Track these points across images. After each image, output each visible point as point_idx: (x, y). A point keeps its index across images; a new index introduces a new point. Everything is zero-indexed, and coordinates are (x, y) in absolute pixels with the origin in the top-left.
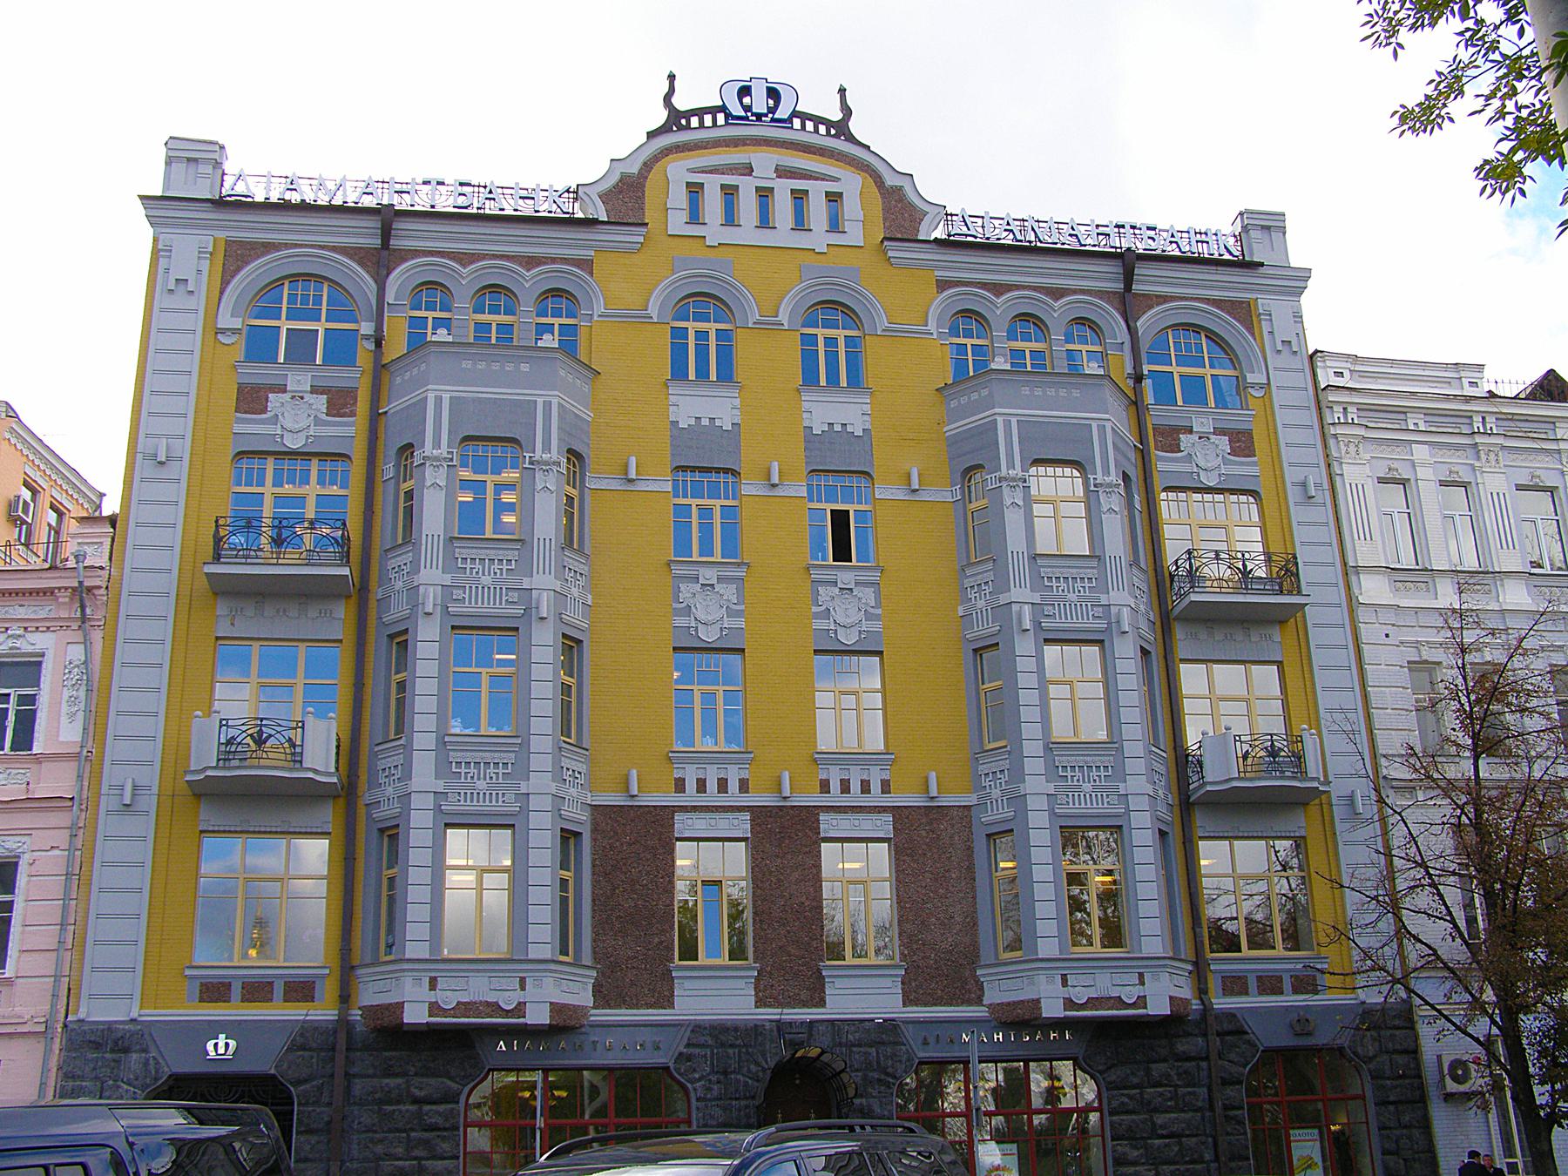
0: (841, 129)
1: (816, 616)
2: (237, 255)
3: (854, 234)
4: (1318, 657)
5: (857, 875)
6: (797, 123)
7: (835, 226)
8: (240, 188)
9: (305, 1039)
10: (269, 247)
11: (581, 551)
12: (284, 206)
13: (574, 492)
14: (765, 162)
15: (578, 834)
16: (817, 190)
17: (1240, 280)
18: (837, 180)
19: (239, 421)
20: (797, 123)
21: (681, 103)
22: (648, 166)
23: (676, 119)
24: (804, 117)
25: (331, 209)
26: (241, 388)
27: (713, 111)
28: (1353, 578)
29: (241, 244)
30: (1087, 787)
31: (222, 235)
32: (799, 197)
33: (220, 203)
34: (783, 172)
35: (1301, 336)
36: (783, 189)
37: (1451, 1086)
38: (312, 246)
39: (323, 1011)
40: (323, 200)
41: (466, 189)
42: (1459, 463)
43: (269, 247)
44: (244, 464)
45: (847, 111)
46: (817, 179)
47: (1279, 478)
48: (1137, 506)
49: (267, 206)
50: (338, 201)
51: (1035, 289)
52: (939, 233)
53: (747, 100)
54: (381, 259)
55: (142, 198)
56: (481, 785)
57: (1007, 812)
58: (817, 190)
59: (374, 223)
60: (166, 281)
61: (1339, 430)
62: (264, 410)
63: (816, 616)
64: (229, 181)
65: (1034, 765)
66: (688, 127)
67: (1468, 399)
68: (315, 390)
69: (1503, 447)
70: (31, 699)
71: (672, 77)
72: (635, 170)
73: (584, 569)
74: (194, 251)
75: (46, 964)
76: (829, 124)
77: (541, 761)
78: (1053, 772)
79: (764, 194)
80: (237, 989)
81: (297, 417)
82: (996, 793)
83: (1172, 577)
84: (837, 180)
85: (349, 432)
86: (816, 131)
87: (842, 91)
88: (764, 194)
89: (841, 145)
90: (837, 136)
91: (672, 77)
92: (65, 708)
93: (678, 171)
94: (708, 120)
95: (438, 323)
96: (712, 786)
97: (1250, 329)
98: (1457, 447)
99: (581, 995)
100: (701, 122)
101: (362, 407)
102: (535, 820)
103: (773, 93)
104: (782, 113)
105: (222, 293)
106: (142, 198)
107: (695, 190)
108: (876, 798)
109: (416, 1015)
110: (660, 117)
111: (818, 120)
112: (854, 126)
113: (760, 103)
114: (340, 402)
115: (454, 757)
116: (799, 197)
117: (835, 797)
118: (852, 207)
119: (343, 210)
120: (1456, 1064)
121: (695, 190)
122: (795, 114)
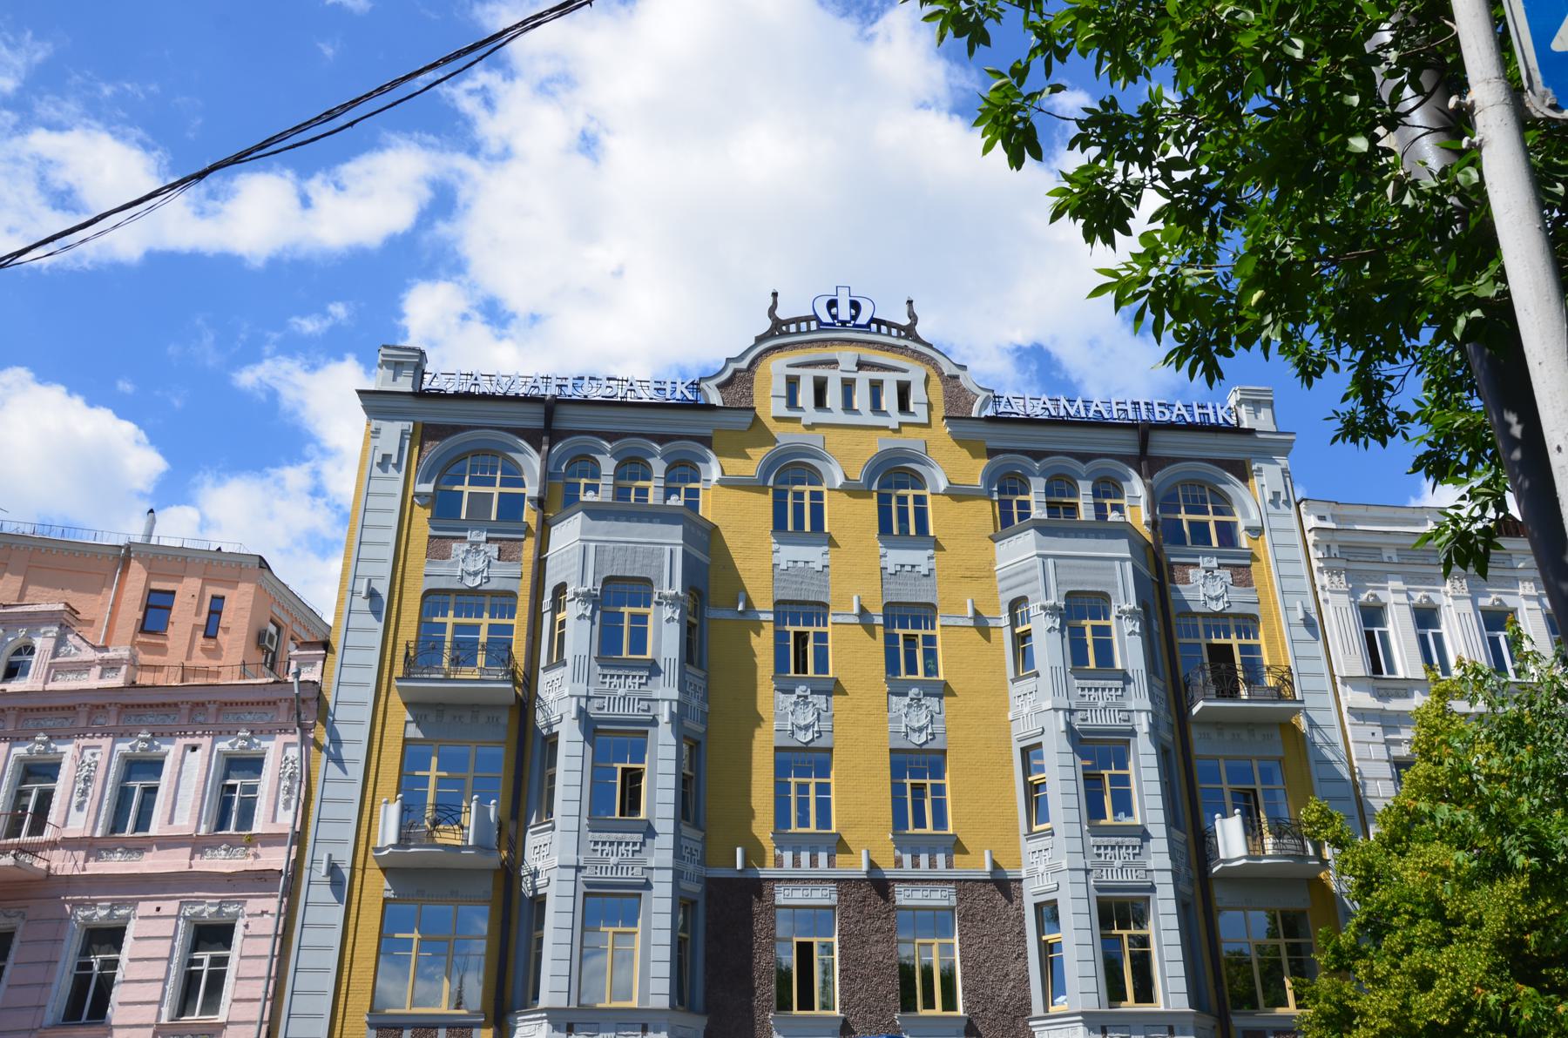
0: (909, 332)
1: (891, 720)
3: (919, 412)
6: (874, 326)
7: (903, 406)
8: (435, 385)
11: (700, 667)
12: (468, 396)
13: (694, 620)
14: (847, 357)
15: (694, 903)
16: (890, 382)
18: (905, 371)
20: (874, 326)
21: (782, 314)
22: (753, 363)
23: (778, 327)
24: (880, 322)
25: (505, 398)
27: (807, 319)
31: (420, 419)
32: (876, 387)
33: (420, 395)
34: (861, 365)
36: (863, 379)
40: (500, 391)
41: (612, 383)
43: (457, 429)
44: (430, 598)
45: (913, 317)
48: (1156, 628)
49: (457, 396)
50: (511, 393)
52: (990, 412)
53: (834, 311)
55: (360, 392)
58: (890, 382)
59: (539, 410)
63: (891, 720)
64: (427, 378)
70: (254, 789)
71: (775, 295)
72: (744, 364)
73: (702, 684)
75: (253, 1012)
79: (848, 386)
82: (1041, 868)
84: (905, 371)
86: (889, 334)
87: (910, 302)
88: (848, 386)
89: (912, 345)
90: (906, 338)
91: (775, 295)
92: (283, 797)
93: (777, 368)
94: (804, 326)
95: (588, 487)
100: (798, 328)
103: (855, 305)
104: (863, 319)
106: (360, 392)
107: (792, 383)
110: (767, 324)
111: (890, 325)
112: (920, 329)
113: (844, 312)
116: (876, 387)
118: (917, 394)
119: (516, 398)
121: (792, 383)
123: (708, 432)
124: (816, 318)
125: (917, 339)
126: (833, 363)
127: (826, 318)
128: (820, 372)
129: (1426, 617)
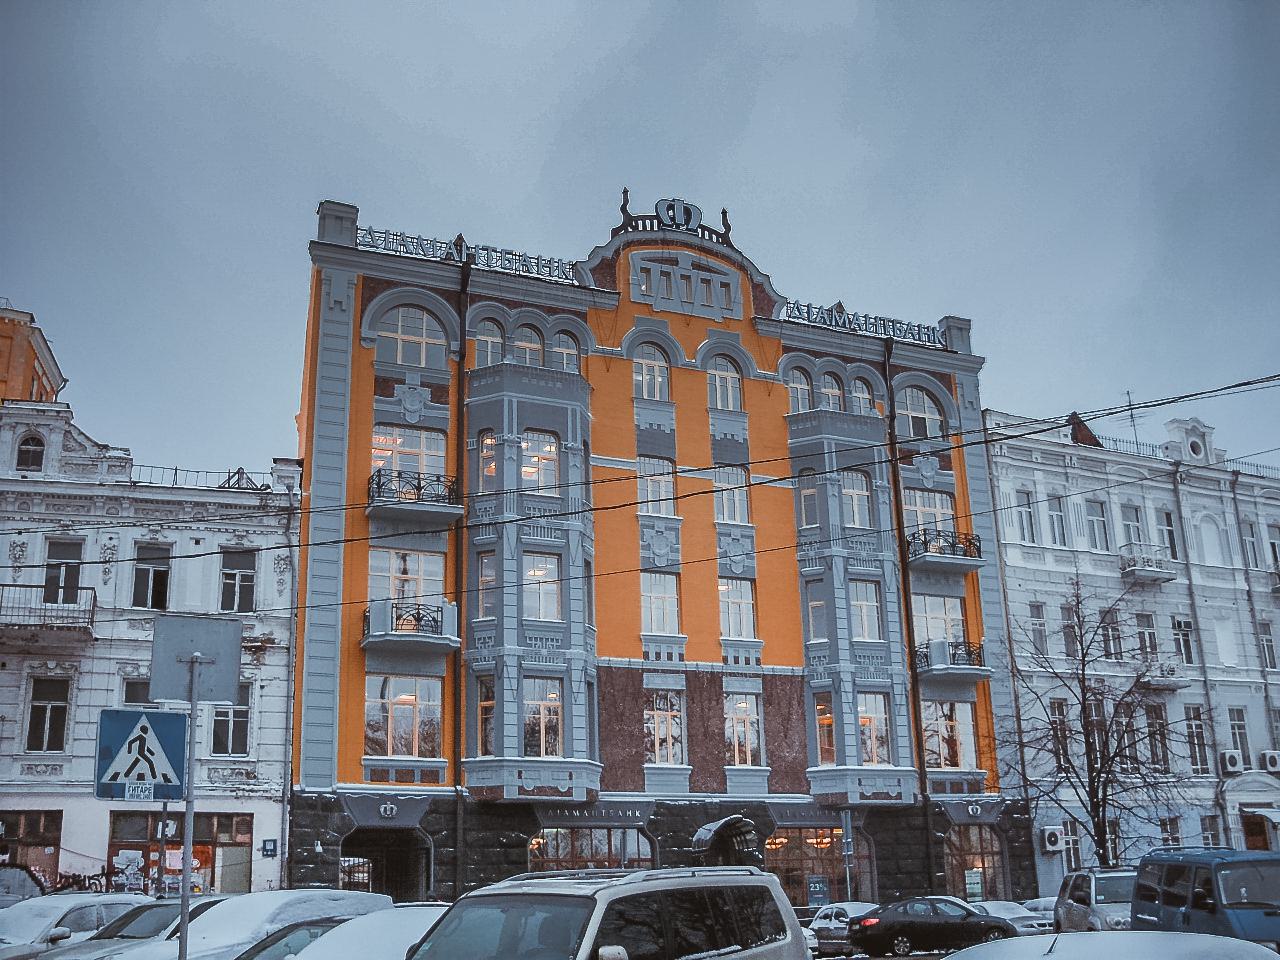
2: (371, 288)
4: (984, 596)
5: (742, 717)
9: (436, 804)
10: (390, 284)
17: (943, 360)
18: (726, 274)
19: (377, 401)
22: (617, 252)
23: (629, 221)
24: (704, 228)
26: (377, 379)
28: (1002, 548)
29: (372, 279)
30: (872, 669)
31: (361, 272)
34: (697, 266)
35: (978, 399)
37: (1050, 848)
38: (417, 286)
39: (445, 789)
42: (1058, 483)
43: (390, 284)
45: (728, 227)
46: (715, 272)
47: (964, 485)
51: (836, 356)
54: (460, 299)
56: (544, 652)
57: (827, 681)
60: (329, 303)
61: (999, 459)
62: (392, 396)
65: (844, 654)
66: (635, 228)
67: (1064, 446)
68: (423, 385)
69: (1189, 492)
74: (345, 283)
76: (718, 235)
77: (576, 639)
78: (854, 658)
80: (392, 775)
81: (412, 401)
83: (909, 543)
84: (726, 274)
85: (448, 412)
86: (711, 238)
87: (724, 213)
90: (722, 243)
96: (664, 656)
97: (950, 390)
98: (1056, 474)
99: (597, 786)
101: (452, 397)
102: (577, 675)
103: (687, 212)
105: (363, 312)
108: (753, 668)
109: (510, 794)
110: (619, 220)
111: (712, 232)
114: (439, 393)
115: (528, 634)
117: (732, 667)
120: (1053, 834)
122: (701, 226)
123: (583, 309)
124: (657, 217)
125: (730, 245)
126: (674, 262)
127: (668, 221)
128: (666, 268)
129: (1056, 500)
